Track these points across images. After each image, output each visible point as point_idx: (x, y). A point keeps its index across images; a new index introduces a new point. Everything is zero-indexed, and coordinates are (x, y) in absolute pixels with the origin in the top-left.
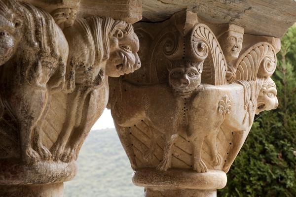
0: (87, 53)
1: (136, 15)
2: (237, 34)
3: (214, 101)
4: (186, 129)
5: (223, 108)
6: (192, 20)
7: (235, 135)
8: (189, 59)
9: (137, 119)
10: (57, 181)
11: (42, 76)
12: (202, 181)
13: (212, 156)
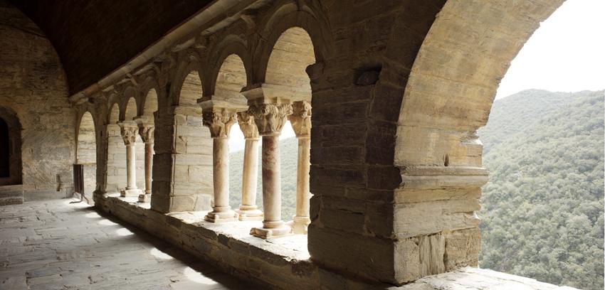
0: (282, 112)
9: (295, 123)
10: (278, 135)
11: (274, 116)
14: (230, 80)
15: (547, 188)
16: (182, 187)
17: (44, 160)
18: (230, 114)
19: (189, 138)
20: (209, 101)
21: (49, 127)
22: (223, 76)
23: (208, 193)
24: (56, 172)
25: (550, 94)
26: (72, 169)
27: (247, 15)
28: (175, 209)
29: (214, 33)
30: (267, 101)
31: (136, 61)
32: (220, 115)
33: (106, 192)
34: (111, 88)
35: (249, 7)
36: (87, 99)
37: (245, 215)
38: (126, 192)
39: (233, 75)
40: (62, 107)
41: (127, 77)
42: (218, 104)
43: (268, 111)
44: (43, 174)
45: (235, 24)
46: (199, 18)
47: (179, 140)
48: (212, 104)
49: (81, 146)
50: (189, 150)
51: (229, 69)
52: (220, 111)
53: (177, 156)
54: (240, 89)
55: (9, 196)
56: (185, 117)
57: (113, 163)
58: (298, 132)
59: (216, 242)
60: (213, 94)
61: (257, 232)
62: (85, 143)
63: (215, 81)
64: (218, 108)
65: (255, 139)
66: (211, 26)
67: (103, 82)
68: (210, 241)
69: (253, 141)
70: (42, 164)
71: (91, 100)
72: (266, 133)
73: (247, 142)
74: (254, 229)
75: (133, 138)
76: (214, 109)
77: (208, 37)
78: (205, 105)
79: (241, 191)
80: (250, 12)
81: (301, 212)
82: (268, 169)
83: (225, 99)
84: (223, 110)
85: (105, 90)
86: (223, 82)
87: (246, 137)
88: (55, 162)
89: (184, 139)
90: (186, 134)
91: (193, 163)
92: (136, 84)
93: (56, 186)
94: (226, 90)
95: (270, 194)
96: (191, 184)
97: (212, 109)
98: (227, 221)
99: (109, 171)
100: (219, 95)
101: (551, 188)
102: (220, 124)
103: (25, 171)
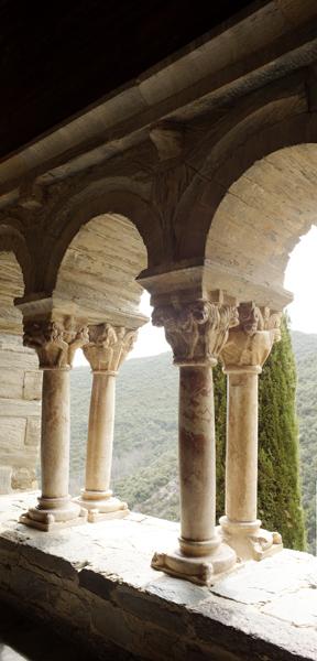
1: (238, 305)
2: (267, 310)
3: (261, 338)
4: (250, 349)
5: (264, 340)
6: (254, 304)
7: (266, 351)
8: (252, 321)
12: (255, 369)
13: (258, 360)
14: (83, 266)
15: (306, 431)
18: (78, 327)
20: (44, 301)
23: (6, 465)
25: (304, 335)
27: (165, 129)
29: (62, 181)
30: (205, 296)
32: (62, 327)
35: (174, 113)
39: (89, 258)
42: (61, 307)
43: (206, 317)
45: (119, 158)
46: (36, 150)
48: (51, 306)
51: (86, 245)
52: (61, 319)
54: (137, 272)
58: (95, 366)
59: (73, 585)
60: (54, 287)
61: (170, 564)
63: (58, 265)
64: (57, 314)
66: (63, 163)
68: (53, 578)
69: (108, 376)
72: (196, 359)
73: (96, 379)
74: (164, 557)
76: (53, 315)
77: (45, 187)
78: (33, 308)
79: (85, 463)
80: (170, 125)
81: (241, 514)
82: (197, 432)
83: (74, 298)
84: (67, 318)
86: (71, 269)
87: (94, 370)
94: (74, 283)
95: (200, 485)
97: (49, 315)
98: (70, 527)
100: (64, 290)
101: (310, 431)
102: (64, 345)
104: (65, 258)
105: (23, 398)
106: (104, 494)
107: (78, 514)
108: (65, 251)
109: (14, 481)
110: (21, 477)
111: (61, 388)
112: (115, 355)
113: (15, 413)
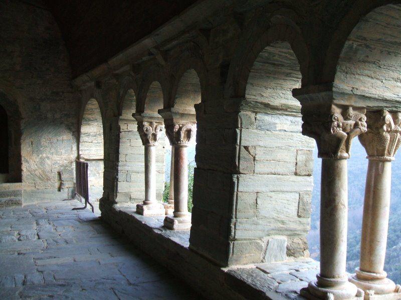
16: (247, 226)
17: (44, 155)
19: (258, 149)
20: (323, 94)
21: (49, 115)
22: (351, 47)
24: (57, 169)
26: (74, 166)
28: (237, 261)
31: (167, 30)
33: (116, 203)
34: (127, 68)
36: (93, 83)
37: (372, 292)
38: (145, 207)
39: (367, 47)
40: (63, 92)
41: (150, 54)
44: (43, 171)
47: (244, 152)
49: (83, 138)
50: (259, 168)
53: (242, 177)
55: (8, 195)
56: (253, 115)
57: (125, 165)
62: (88, 135)
65: (388, 158)
67: (114, 61)
70: (42, 159)
71: (98, 85)
75: (154, 136)
85: (117, 72)
88: (56, 158)
89: (252, 151)
90: (254, 144)
91: (264, 189)
92: (163, 63)
93: (57, 185)
96: (260, 222)
99: (121, 176)
103: (24, 167)
104: (344, 50)
105: (296, 174)
106: (378, 275)
107: (355, 294)
108: (344, 43)
109: (288, 249)
110: (296, 246)
111: (339, 176)
112: (392, 141)
113: (288, 189)
